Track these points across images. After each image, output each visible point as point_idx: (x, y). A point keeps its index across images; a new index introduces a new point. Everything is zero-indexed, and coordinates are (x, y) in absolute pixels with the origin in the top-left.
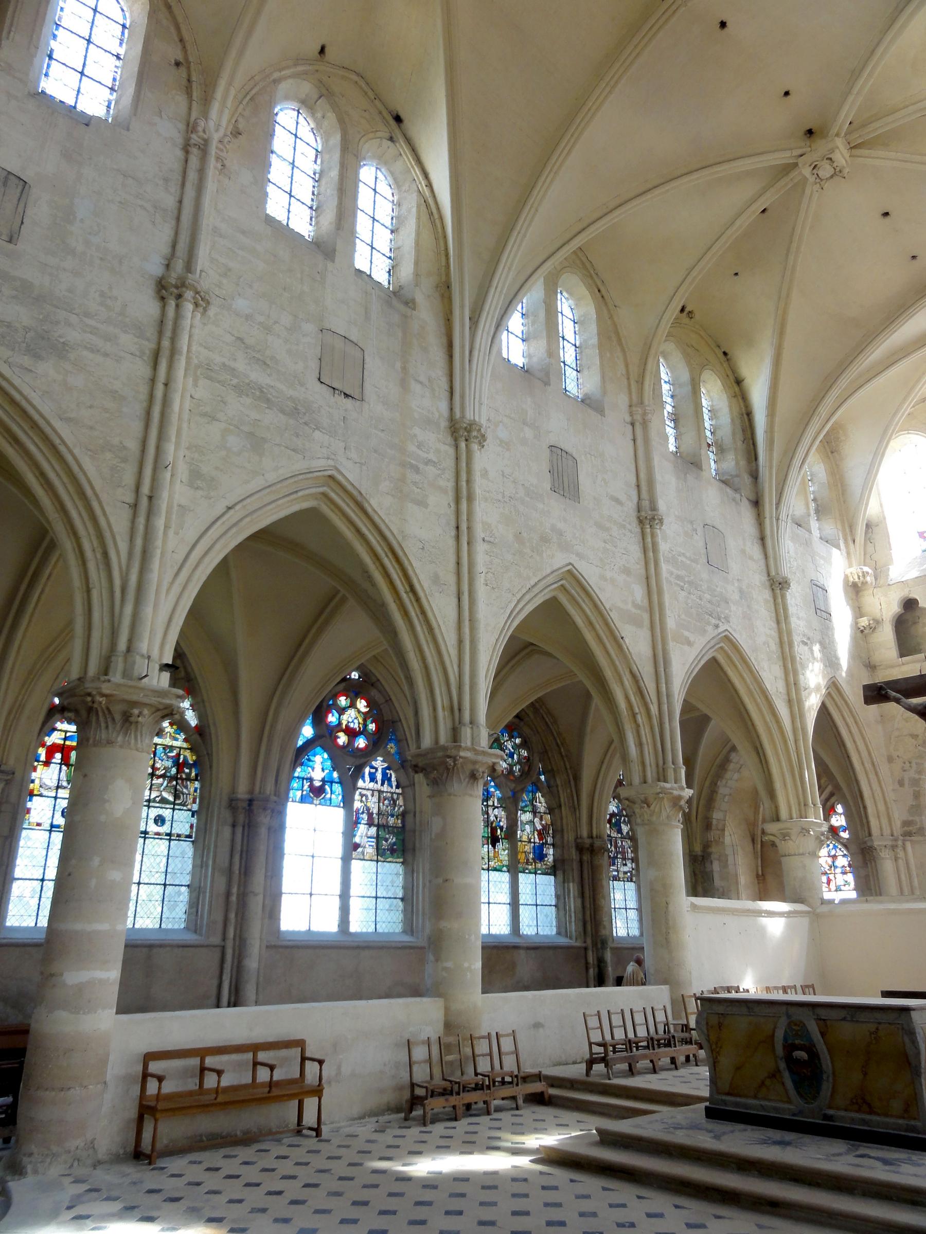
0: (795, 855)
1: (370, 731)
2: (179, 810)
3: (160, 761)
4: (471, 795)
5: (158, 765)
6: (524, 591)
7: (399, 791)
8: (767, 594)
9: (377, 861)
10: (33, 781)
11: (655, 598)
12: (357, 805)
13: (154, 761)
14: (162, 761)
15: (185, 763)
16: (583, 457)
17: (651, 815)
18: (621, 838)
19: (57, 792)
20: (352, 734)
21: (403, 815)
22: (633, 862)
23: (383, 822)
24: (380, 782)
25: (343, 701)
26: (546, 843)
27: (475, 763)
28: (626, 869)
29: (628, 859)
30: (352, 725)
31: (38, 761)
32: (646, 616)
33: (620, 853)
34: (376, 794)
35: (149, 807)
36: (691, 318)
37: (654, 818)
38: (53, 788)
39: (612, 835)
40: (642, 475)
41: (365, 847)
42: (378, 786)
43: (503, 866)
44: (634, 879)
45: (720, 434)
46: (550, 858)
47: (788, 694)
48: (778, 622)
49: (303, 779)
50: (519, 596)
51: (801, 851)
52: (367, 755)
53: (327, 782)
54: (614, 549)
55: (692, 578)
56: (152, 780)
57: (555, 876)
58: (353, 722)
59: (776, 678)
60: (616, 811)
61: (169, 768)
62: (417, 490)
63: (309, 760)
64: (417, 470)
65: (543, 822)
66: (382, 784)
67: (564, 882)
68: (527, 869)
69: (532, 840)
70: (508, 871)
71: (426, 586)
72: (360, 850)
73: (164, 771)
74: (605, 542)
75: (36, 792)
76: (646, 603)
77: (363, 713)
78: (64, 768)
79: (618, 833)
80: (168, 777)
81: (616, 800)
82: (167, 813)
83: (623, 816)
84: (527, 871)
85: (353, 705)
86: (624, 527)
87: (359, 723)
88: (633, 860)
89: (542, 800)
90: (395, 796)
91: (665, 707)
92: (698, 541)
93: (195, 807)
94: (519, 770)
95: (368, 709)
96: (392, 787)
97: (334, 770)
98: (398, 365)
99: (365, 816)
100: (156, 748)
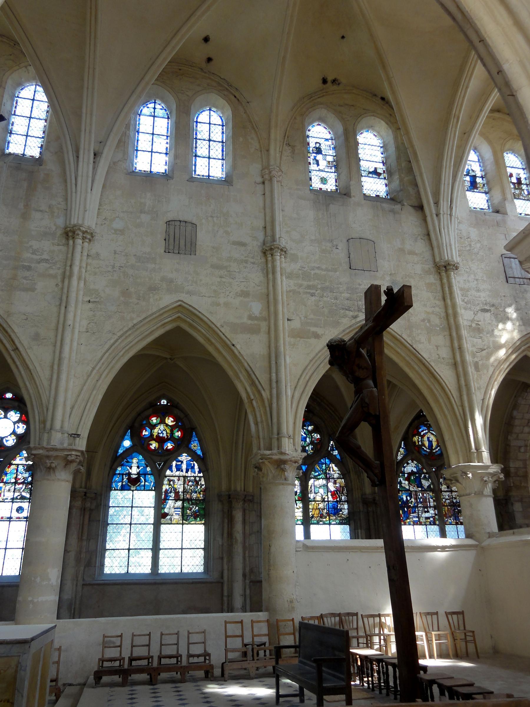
0: (464, 496)
1: (177, 438)
3: (21, 474)
4: (48, 480)
5: (19, 477)
6: (126, 329)
7: (201, 475)
8: (432, 279)
9: (183, 524)
11: (272, 309)
12: (165, 487)
14: (22, 474)
16: (204, 221)
17: (263, 477)
18: (421, 491)
20: (161, 441)
21: (205, 491)
22: (435, 509)
23: (188, 496)
24: (184, 471)
25: (154, 420)
26: (341, 500)
27: (48, 457)
28: (427, 515)
29: (430, 507)
30: (161, 435)
32: (264, 325)
33: (421, 503)
34: (182, 479)
35: (13, 502)
36: (339, 84)
37: (265, 479)
39: (411, 489)
40: (268, 218)
41: (172, 515)
42: (184, 473)
43: (298, 520)
44: (437, 522)
45: (389, 161)
46: (346, 512)
47: (454, 358)
48: (444, 299)
49: (123, 474)
50: (119, 334)
51: (468, 492)
52: (174, 454)
53: (142, 474)
54: (231, 280)
55: (327, 284)
57: (349, 525)
58: (162, 433)
59: (437, 347)
60: (415, 470)
61: (26, 478)
62: (25, 281)
63: (128, 462)
64: (29, 268)
65: (337, 485)
66: (187, 471)
67: (355, 529)
68: (321, 521)
69: (326, 500)
70: (302, 524)
71: (25, 343)
72: (168, 517)
73: (23, 480)
74: (221, 277)
76: (265, 314)
77: (170, 426)
79: (418, 487)
80: (26, 483)
81: (415, 462)
83: (424, 473)
84: (321, 523)
85: (162, 422)
86: (246, 262)
87: (167, 433)
88: (435, 508)
89: (335, 468)
90: (198, 479)
91: (274, 391)
92: (341, 254)
94: (312, 449)
95: (174, 423)
96: (195, 473)
97: (147, 466)
98: (21, 206)
99: (173, 495)
100: (18, 467)
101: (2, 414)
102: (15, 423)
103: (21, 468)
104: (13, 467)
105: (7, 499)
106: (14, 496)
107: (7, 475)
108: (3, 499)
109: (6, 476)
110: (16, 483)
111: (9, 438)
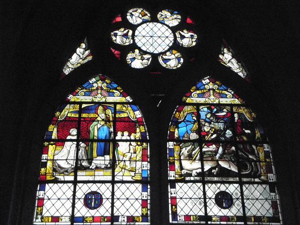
2: (249, 183)
3: (207, 124)
10: (45, 165)
13: (199, 124)
14: (210, 123)
15: (244, 123)
19: (76, 176)
31: (50, 140)
35: (204, 183)
38: (70, 170)
56: (201, 148)
73: (215, 136)
75: (48, 178)
78: (82, 144)
80: (222, 142)
82: (232, 189)
93: (272, 177)
100: (198, 110)
101: (147, 15)
102: (174, 29)
103: (204, 111)
104: (188, 109)
105: (190, 175)
106: (202, 168)
107: (180, 125)
108: (181, 175)
109: (178, 128)
110: (201, 141)
111: (168, 56)
